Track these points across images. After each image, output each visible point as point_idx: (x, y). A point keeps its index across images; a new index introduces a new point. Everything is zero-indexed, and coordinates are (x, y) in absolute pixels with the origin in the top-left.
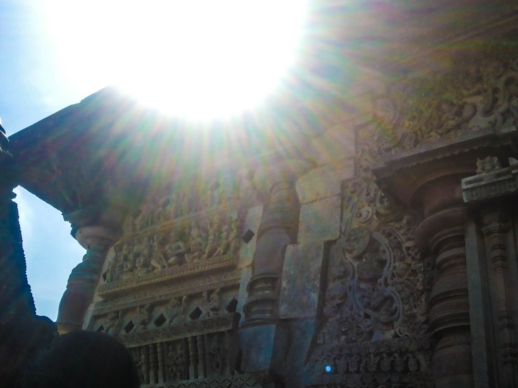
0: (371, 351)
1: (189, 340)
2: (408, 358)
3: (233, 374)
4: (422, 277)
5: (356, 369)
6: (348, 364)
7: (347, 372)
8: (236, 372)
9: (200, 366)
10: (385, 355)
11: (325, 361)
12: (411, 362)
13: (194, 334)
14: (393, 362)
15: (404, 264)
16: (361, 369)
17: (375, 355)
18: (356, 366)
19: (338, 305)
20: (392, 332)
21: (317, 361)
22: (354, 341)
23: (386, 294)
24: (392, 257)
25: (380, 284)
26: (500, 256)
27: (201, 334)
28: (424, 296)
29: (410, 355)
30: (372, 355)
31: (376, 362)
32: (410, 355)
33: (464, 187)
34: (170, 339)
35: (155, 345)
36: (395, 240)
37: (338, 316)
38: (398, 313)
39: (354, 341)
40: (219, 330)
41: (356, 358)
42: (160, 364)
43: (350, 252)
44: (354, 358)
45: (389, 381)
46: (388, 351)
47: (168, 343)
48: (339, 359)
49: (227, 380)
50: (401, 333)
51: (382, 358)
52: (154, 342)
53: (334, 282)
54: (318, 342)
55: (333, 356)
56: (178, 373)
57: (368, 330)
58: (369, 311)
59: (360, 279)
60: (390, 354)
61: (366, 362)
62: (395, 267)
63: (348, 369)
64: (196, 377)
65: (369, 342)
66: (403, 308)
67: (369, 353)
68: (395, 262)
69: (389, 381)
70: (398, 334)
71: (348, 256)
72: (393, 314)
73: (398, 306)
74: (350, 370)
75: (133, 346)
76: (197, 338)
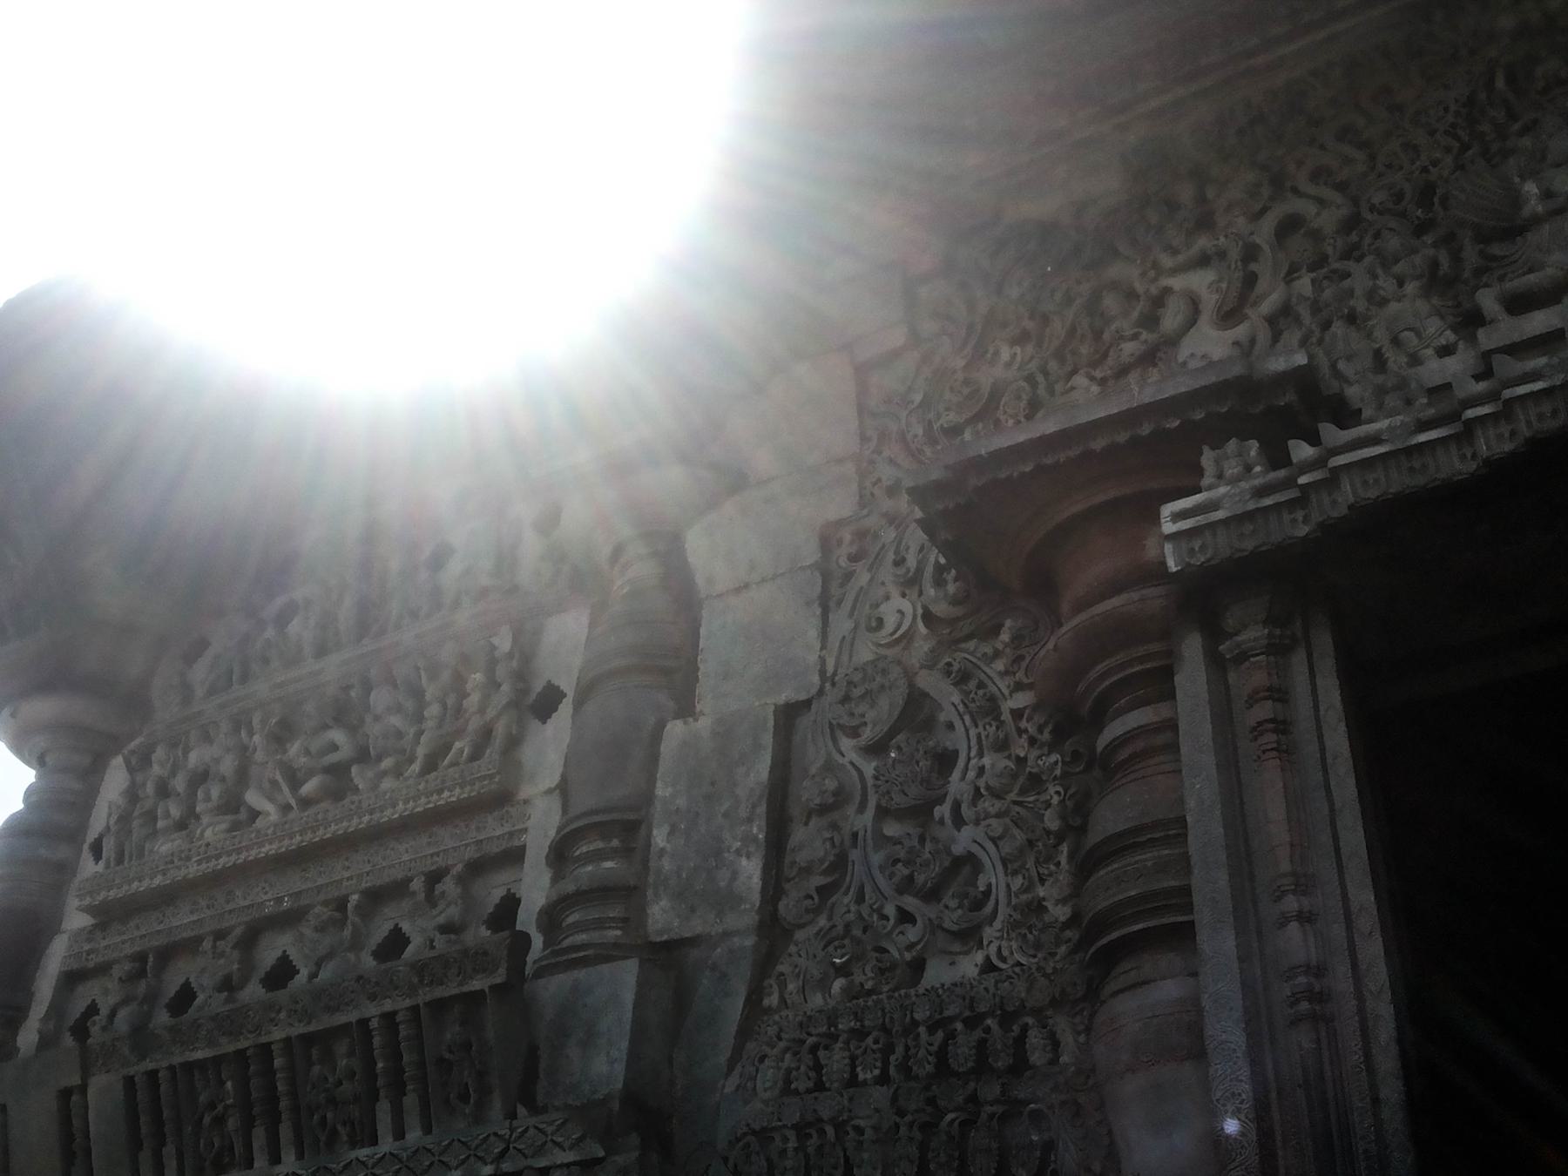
0: (916, 1016)
1: (374, 1024)
2: (1025, 1029)
3: (512, 1115)
4: (1058, 793)
5: (877, 1072)
6: (853, 1059)
7: (853, 1081)
8: (522, 1111)
9: (410, 1101)
10: (959, 1026)
11: (788, 1056)
12: (1035, 1038)
13: (388, 1006)
14: (982, 1044)
15: (1009, 757)
16: (892, 1071)
17: (932, 1030)
18: (878, 1064)
19: (820, 890)
20: (979, 957)
21: (762, 1059)
22: (870, 993)
23: (958, 850)
24: (974, 742)
25: (942, 822)
26: (1269, 689)
27: (408, 1003)
28: (1065, 848)
29: (1030, 1020)
30: (922, 1029)
31: (934, 1048)
32: (1030, 1020)
33: (1168, 528)
34: (312, 1028)
35: (266, 1050)
36: (981, 692)
37: (822, 922)
38: (993, 897)
39: (870, 993)
40: (465, 989)
41: (876, 1042)
42: (284, 1104)
43: (854, 732)
44: (870, 1040)
45: (973, 1099)
46: (967, 1013)
47: (308, 1040)
48: (826, 1048)
49: (495, 1134)
50: (1004, 960)
51: (951, 1035)
52: (264, 1039)
53: (806, 824)
54: (766, 1002)
55: (811, 1040)
56: (339, 1127)
57: (908, 956)
58: (911, 903)
59: (883, 813)
60: (972, 1022)
61: (907, 1048)
62: (981, 770)
63: (854, 1075)
64: (399, 1134)
65: (912, 991)
66: (1008, 886)
67: (915, 1023)
68: (981, 755)
69: (973, 1099)
70: (995, 961)
71: (846, 743)
72: (978, 905)
73: (993, 881)
74: (861, 1077)
75: (199, 1055)
76: (399, 1018)
